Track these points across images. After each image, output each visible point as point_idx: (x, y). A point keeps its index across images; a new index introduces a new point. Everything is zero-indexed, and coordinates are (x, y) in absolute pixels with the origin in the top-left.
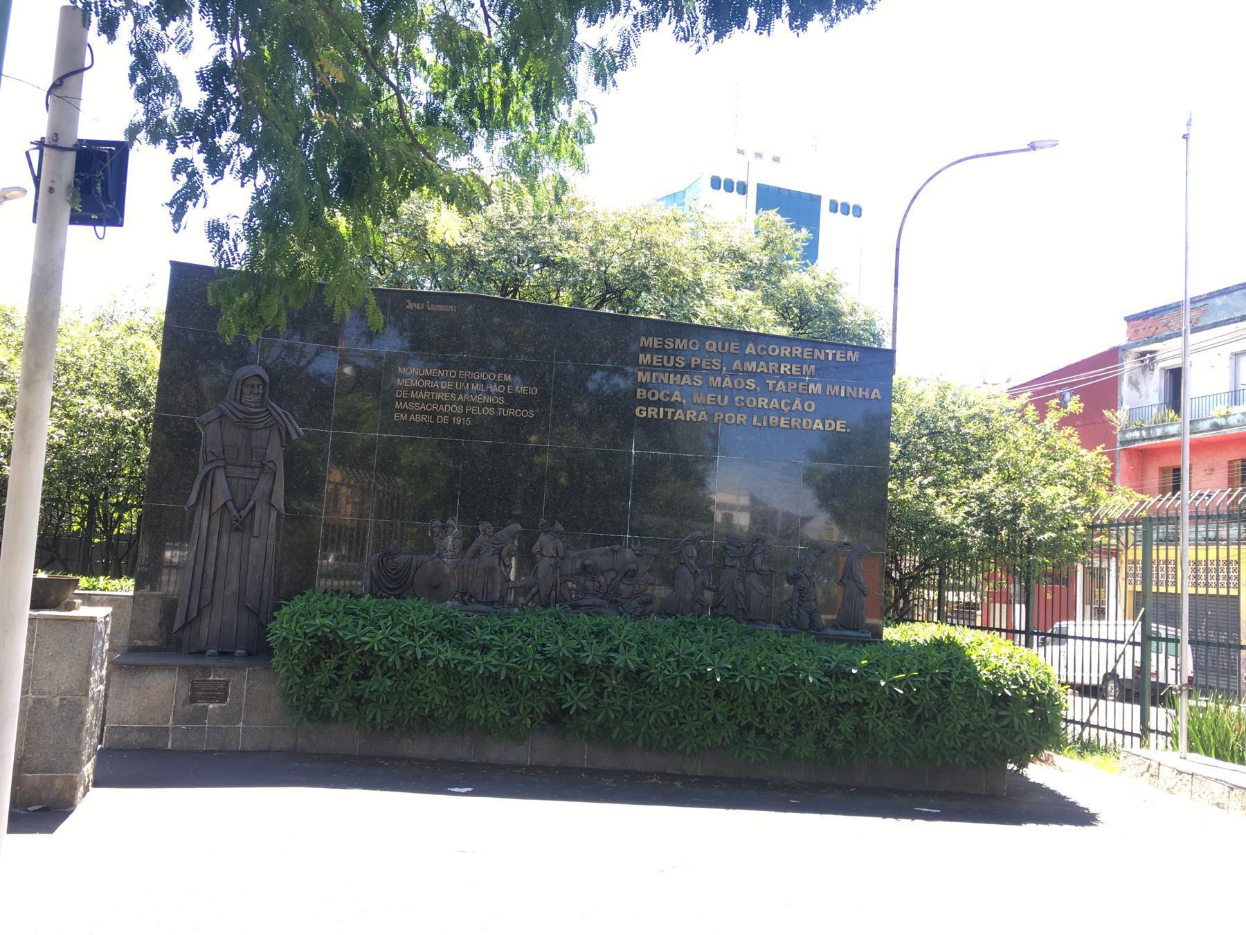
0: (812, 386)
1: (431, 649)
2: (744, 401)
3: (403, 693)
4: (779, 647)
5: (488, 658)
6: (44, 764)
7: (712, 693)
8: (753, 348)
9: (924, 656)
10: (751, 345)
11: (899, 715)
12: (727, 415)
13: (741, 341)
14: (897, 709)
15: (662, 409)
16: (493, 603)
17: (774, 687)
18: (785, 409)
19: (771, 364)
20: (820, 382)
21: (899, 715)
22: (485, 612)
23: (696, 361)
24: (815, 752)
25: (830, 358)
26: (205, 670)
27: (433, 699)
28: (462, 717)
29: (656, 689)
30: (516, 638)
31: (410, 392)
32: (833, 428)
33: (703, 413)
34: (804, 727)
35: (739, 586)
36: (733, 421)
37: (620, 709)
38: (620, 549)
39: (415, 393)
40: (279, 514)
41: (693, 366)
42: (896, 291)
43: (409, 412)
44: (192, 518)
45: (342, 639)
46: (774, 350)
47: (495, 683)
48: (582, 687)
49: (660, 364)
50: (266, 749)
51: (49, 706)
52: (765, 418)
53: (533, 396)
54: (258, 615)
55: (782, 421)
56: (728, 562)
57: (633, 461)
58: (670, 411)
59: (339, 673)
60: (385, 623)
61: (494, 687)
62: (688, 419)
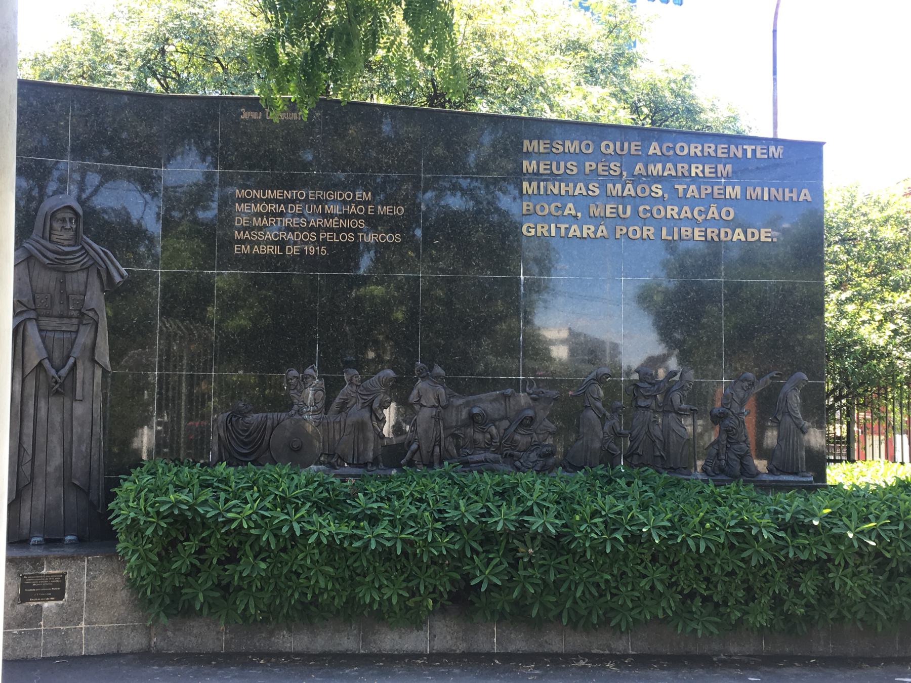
0: (729, 189)
1: (309, 522)
2: (651, 211)
3: (279, 577)
4: (719, 499)
5: (379, 530)
7: (647, 557)
8: (658, 148)
9: (893, 500)
10: (654, 144)
11: (869, 572)
12: (631, 229)
13: (642, 140)
14: (865, 564)
15: (553, 226)
16: (365, 465)
17: (721, 546)
18: (699, 219)
19: (679, 166)
20: (739, 184)
21: (869, 572)
22: (359, 476)
24: (772, 620)
25: (749, 155)
26: (36, 562)
27: (317, 582)
28: (352, 601)
29: (581, 557)
30: (407, 504)
32: (756, 238)
33: (602, 227)
34: (758, 591)
36: (638, 236)
37: (540, 582)
38: (512, 393)
40: (105, 372)
42: (775, 80)
43: (252, 243)
45: (203, 517)
46: (682, 148)
47: (388, 559)
48: (492, 559)
49: (549, 172)
50: (115, 651)
52: (676, 229)
53: (400, 216)
54: (87, 494)
55: (697, 233)
56: (642, 403)
57: (522, 288)
59: (201, 557)
60: (252, 495)
61: (388, 564)
62: (585, 235)
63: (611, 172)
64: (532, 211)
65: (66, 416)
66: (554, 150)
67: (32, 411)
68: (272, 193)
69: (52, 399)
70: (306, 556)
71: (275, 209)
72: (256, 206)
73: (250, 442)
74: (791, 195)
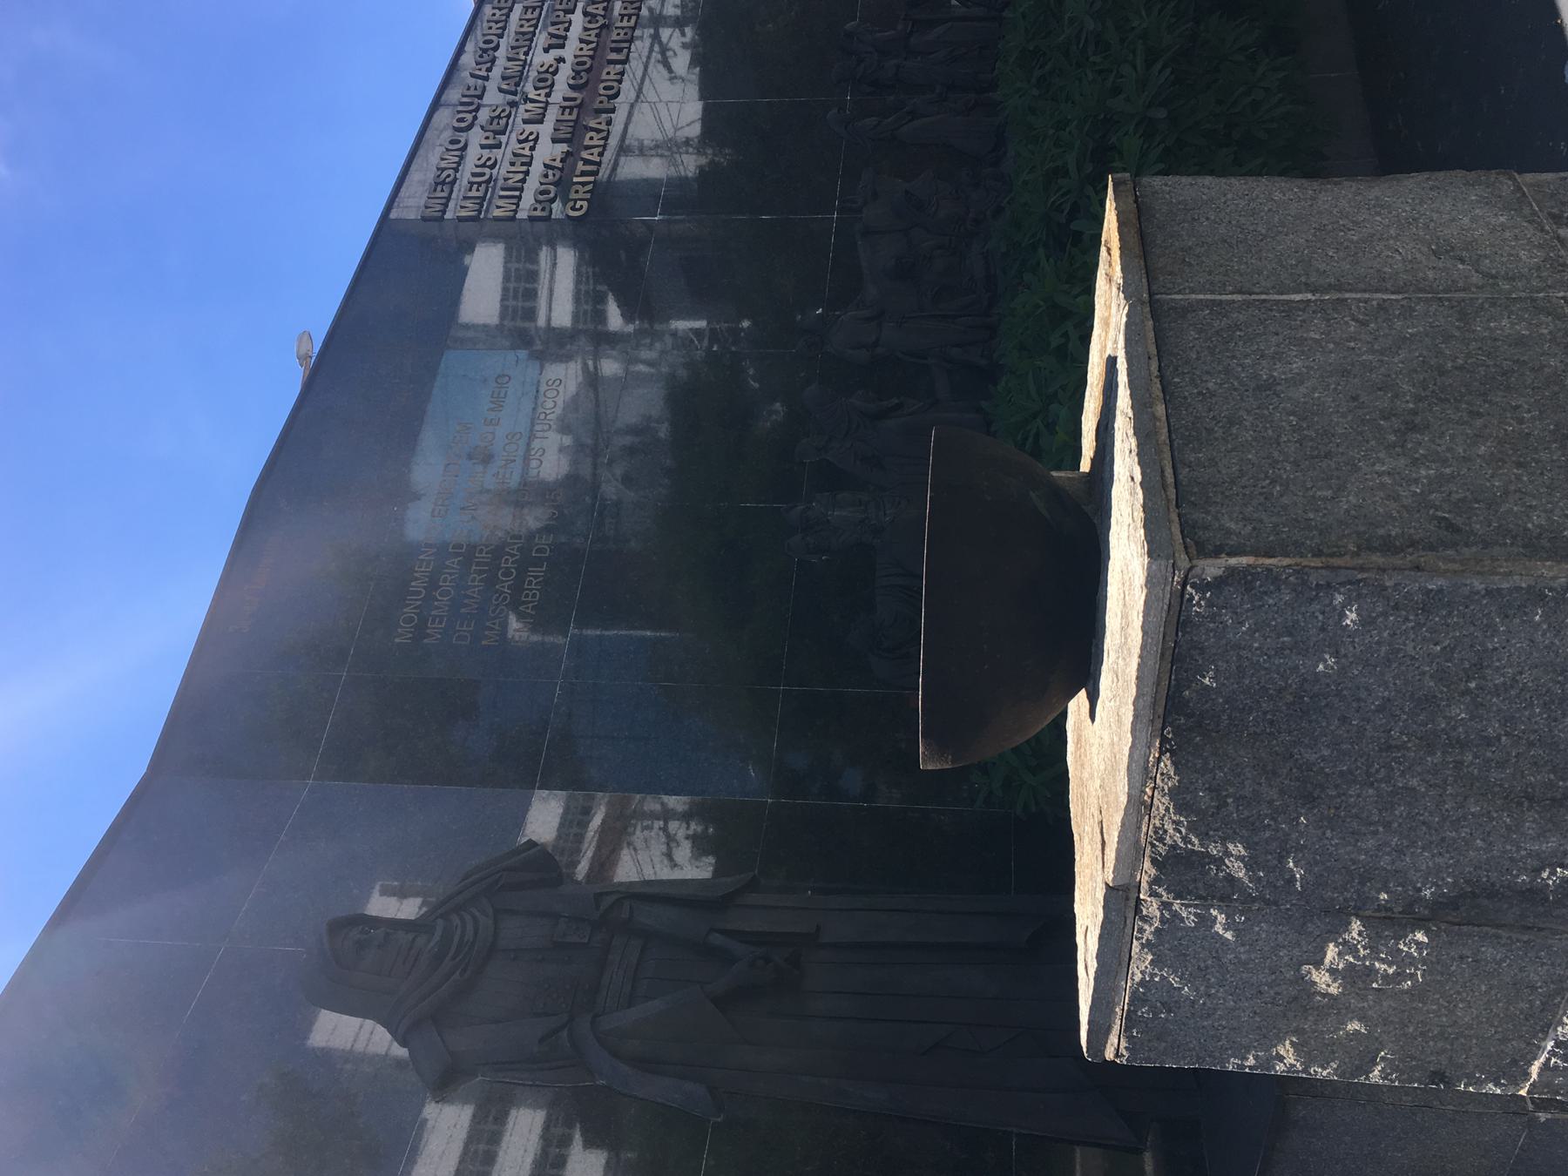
15: (575, 180)
58: (580, 166)
71: (451, 574)
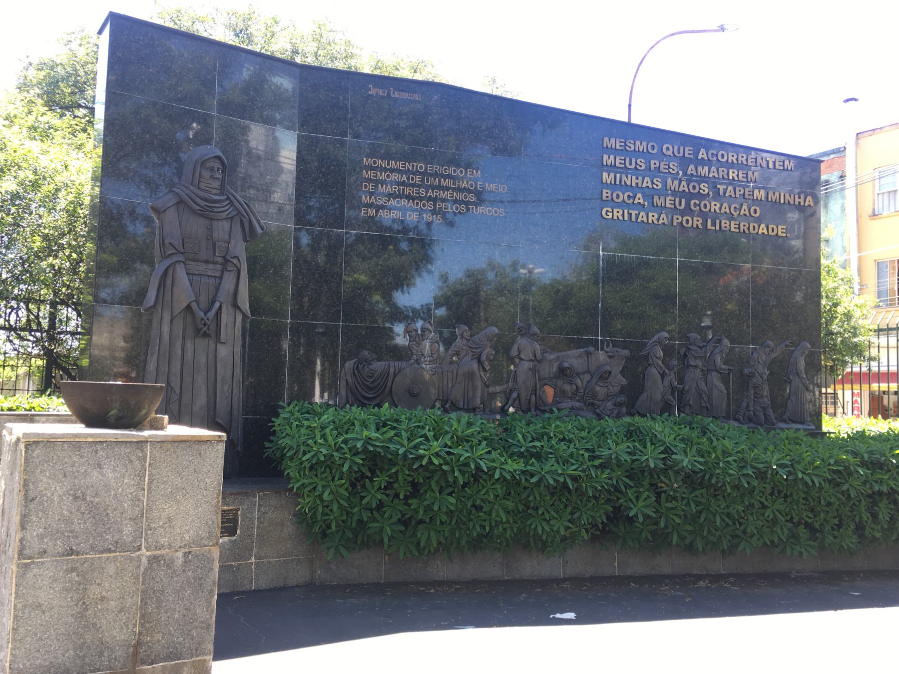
6: (168, 648)
15: (626, 211)
20: (763, 188)
23: (655, 164)
31: (376, 186)
32: (775, 232)
33: (663, 216)
35: (702, 385)
36: (690, 225)
39: (382, 186)
40: (245, 316)
41: (652, 168)
44: (150, 321)
46: (723, 156)
49: (623, 166)
50: (282, 585)
51: (169, 564)
55: (733, 226)
57: (601, 262)
58: (634, 213)
63: (671, 170)
64: (610, 198)
65: (211, 357)
66: (627, 148)
67: (180, 352)
68: (396, 164)
69: (198, 340)
70: (487, 492)
72: (381, 174)
73: (374, 388)
74: (800, 200)
